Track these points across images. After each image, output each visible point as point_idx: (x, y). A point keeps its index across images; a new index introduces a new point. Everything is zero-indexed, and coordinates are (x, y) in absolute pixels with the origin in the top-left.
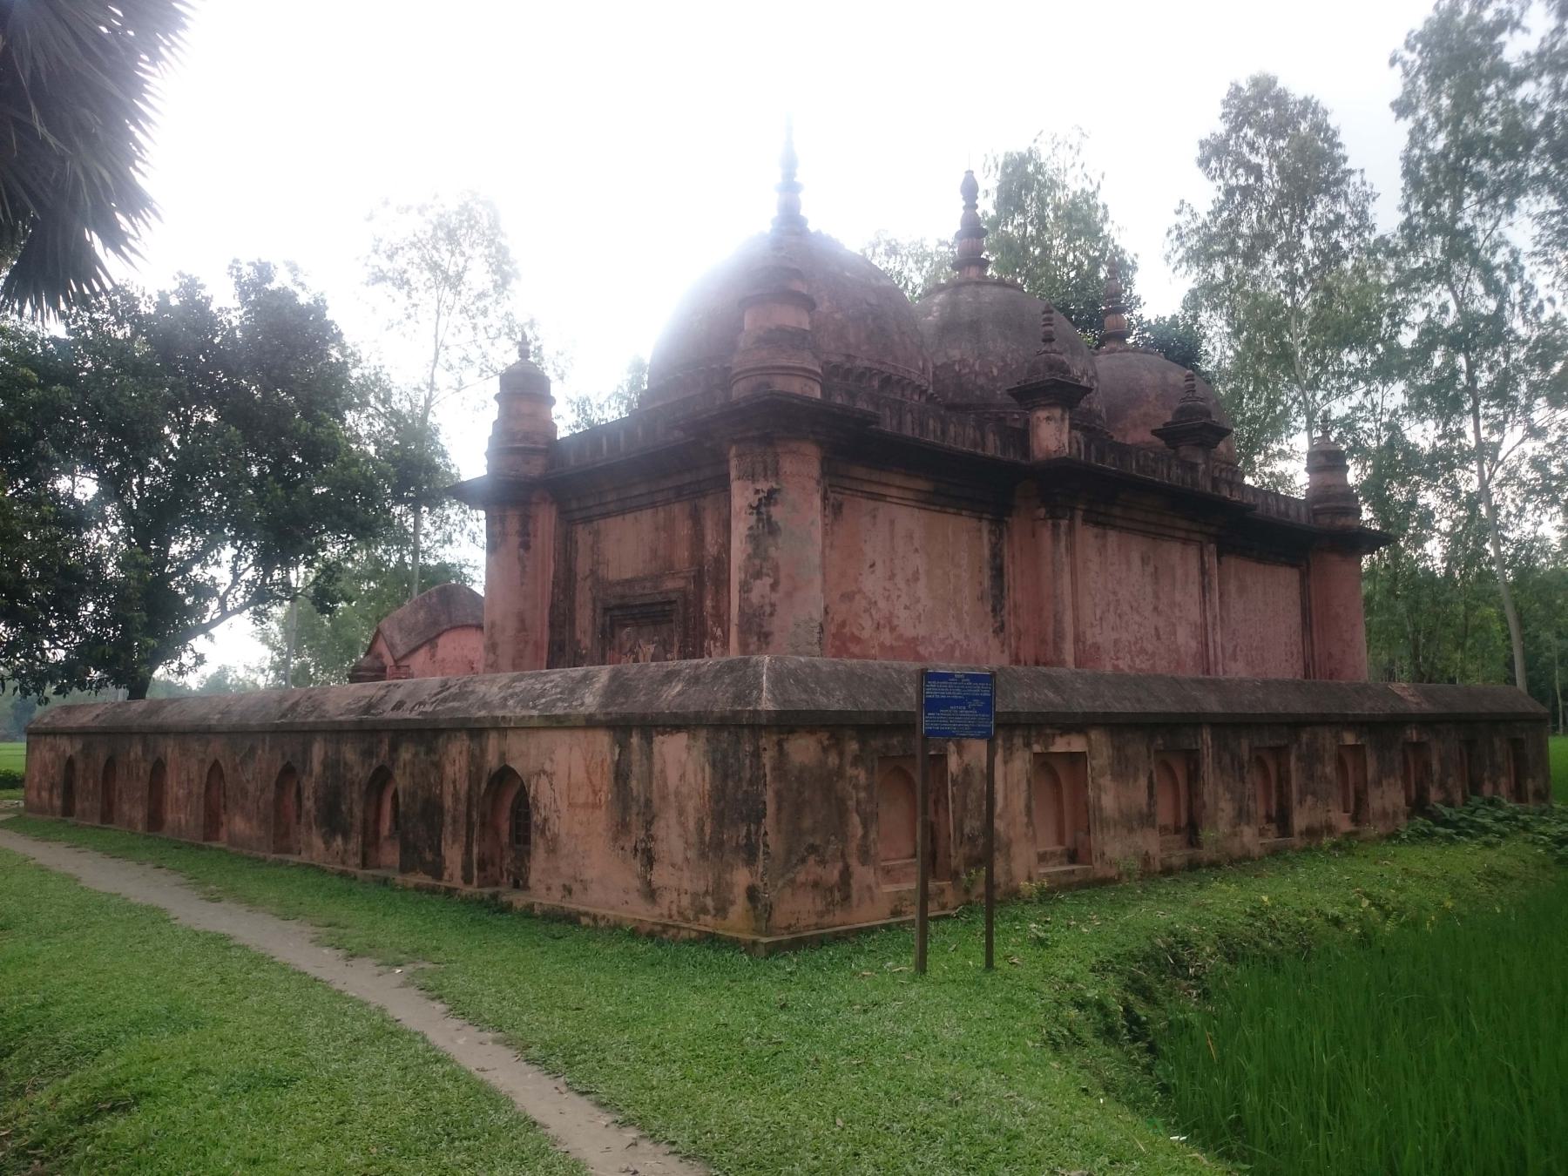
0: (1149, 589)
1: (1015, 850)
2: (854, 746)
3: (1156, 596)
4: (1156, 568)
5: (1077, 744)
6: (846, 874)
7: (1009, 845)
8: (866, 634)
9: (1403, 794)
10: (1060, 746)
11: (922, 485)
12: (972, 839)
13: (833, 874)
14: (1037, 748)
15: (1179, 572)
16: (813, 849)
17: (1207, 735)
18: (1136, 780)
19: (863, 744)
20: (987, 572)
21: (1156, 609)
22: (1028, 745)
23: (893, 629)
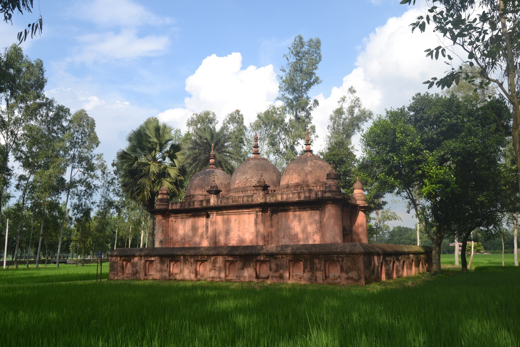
0: (237, 226)
1: (141, 273)
2: (119, 259)
3: (239, 227)
4: (239, 221)
5: (153, 259)
6: (117, 273)
7: (140, 272)
8: (179, 241)
9: (255, 272)
10: (150, 259)
11: (190, 214)
12: (134, 271)
13: (116, 273)
14: (146, 259)
15: (247, 221)
16: (114, 270)
17: (182, 257)
18: (164, 264)
19: (120, 258)
20: (205, 227)
21: (239, 230)
22: (144, 259)
23: (185, 240)
